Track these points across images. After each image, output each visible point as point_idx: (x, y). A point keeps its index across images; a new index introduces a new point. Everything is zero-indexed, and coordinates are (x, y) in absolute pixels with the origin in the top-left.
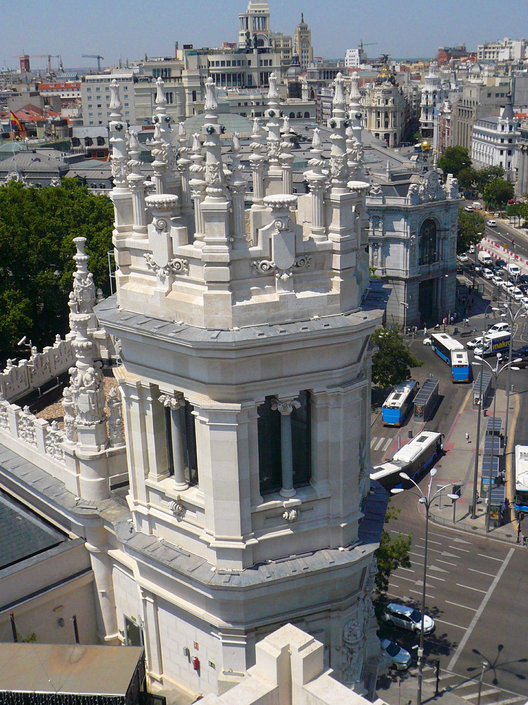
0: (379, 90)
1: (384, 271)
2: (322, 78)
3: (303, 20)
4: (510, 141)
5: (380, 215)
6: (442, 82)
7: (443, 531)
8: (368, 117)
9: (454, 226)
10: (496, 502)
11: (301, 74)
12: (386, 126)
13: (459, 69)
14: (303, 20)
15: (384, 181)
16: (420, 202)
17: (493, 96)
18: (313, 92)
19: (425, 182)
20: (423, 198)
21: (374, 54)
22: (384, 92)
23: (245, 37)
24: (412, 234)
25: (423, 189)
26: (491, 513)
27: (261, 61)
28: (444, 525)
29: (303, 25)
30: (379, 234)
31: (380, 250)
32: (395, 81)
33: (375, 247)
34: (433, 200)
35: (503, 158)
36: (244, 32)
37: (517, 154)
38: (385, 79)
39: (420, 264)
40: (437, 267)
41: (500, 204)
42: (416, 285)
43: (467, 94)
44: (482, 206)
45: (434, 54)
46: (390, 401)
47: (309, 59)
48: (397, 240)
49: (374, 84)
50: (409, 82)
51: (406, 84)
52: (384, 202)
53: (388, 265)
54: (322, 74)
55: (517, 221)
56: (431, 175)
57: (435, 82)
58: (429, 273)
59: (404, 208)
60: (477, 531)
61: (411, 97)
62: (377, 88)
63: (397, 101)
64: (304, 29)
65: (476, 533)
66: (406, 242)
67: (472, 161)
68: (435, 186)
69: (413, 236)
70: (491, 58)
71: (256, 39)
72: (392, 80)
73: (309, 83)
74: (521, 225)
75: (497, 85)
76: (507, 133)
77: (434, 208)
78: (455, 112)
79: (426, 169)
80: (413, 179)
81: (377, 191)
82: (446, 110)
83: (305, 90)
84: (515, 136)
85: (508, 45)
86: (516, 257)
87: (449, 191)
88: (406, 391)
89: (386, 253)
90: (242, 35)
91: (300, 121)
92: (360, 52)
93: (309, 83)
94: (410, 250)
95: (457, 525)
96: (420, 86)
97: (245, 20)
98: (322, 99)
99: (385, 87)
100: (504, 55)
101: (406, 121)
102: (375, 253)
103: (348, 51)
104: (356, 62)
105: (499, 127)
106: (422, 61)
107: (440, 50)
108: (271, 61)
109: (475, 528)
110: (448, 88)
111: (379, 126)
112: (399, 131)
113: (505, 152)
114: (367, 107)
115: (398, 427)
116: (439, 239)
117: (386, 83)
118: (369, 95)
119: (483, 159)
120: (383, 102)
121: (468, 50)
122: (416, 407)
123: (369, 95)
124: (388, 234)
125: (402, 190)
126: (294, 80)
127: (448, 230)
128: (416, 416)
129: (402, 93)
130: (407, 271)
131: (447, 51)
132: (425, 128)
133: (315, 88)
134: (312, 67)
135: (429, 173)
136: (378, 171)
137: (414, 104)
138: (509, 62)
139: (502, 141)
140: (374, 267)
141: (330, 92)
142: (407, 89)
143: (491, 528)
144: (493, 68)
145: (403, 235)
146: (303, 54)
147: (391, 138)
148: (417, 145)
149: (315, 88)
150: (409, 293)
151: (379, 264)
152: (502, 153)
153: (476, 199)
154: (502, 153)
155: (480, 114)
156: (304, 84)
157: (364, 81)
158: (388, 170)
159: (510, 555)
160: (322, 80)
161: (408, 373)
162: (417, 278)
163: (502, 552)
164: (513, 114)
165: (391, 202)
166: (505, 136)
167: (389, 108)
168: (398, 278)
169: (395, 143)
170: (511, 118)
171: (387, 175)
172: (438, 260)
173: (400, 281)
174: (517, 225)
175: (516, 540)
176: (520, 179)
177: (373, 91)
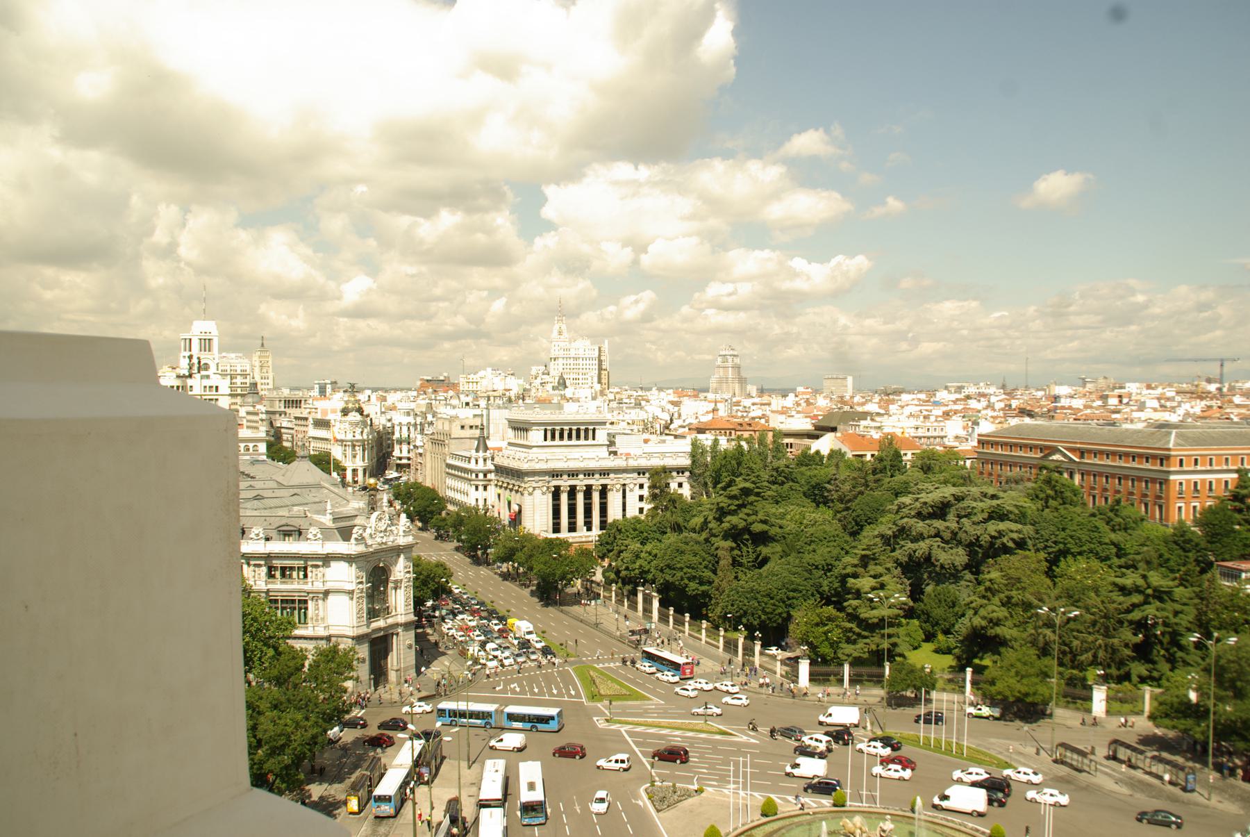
3: (263, 345)
4: (485, 476)
5: (320, 563)
13: (436, 400)
14: (263, 345)
15: (325, 525)
17: (467, 427)
18: (271, 423)
22: (351, 424)
23: (187, 360)
27: (205, 387)
30: (319, 586)
32: (363, 412)
35: (481, 494)
36: (187, 354)
37: (491, 488)
49: (340, 414)
50: (382, 413)
53: (330, 621)
54: (283, 402)
59: (347, 555)
62: (343, 419)
71: (199, 362)
80: (358, 521)
81: (315, 535)
82: (418, 443)
87: (401, 533)
90: (184, 357)
97: (188, 341)
105: (473, 461)
107: (422, 380)
108: (217, 387)
113: (481, 488)
124: (328, 586)
125: (346, 534)
132: (398, 462)
136: (318, 512)
138: (491, 393)
139: (477, 476)
152: (477, 488)
154: (477, 488)
157: (329, 412)
158: (329, 511)
167: (357, 441)
171: (329, 517)
173: (345, 639)
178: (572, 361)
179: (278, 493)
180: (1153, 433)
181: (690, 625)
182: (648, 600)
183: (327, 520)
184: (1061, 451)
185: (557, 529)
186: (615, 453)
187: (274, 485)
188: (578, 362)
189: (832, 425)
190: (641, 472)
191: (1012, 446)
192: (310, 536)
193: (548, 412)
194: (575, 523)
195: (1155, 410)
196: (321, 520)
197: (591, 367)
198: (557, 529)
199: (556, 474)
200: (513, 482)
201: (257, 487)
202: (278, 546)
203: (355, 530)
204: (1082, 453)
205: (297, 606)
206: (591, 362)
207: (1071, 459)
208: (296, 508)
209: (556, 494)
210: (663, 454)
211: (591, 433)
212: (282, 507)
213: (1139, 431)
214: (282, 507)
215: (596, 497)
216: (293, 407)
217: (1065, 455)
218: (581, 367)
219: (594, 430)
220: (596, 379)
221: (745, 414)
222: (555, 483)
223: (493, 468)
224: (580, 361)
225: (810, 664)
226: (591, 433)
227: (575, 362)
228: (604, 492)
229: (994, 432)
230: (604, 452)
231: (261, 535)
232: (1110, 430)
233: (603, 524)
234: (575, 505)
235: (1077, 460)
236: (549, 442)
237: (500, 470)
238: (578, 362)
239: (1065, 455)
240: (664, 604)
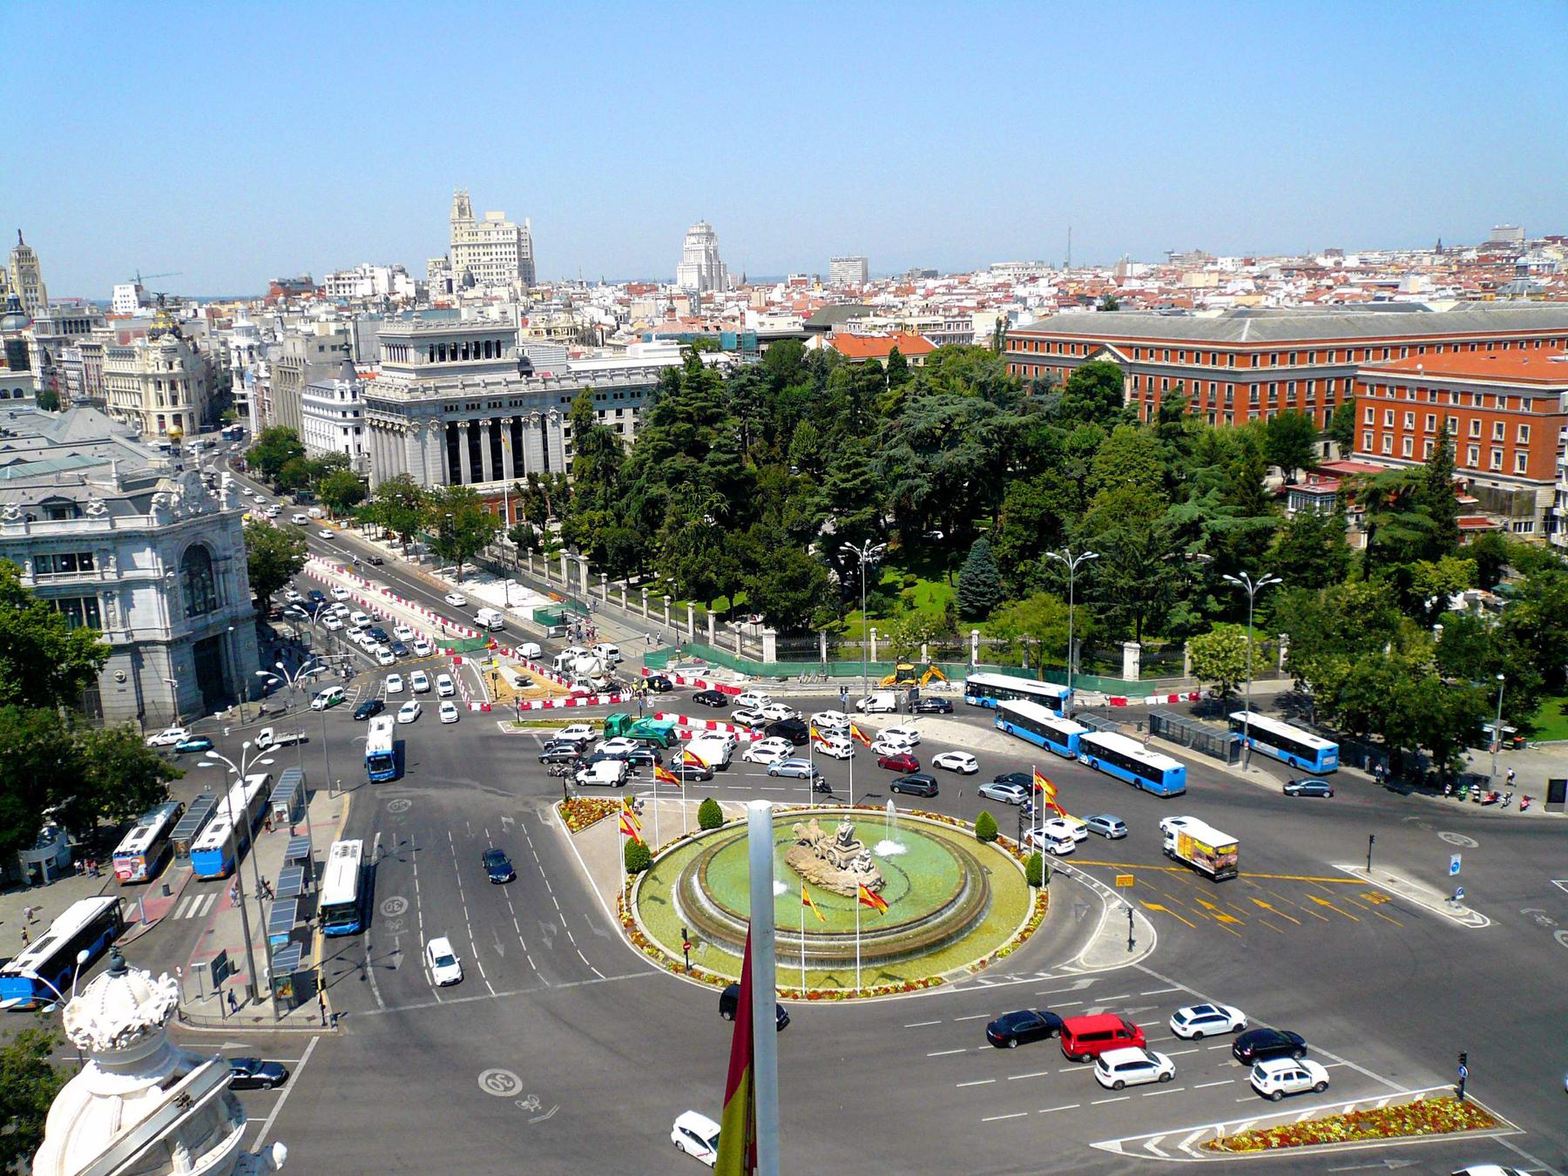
0: (156, 348)
1: (129, 634)
2: (62, 332)
4: (356, 414)
6: (262, 332)
7: (191, 1036)
8: (143, 391)
9: (239, 550)
10: (284, 969)
11: (24, 327)
12: (174, 401)
13: (288, 312)
16: (176, 520)
17: (328, 349)
19: (180, 488)
20: (179, 513)
21: (152, 289)
22: (164, 350)
24: (166, 571)
25: (177, 499)
26: (281, 988)
28: (207, 1026)
29: (22, 248)
30: (111, 576)
31: (117, 601)
32: (181, 333)
33: (109, 598)
34: (197, 514)
35: (350, 439)
38: (163, 331)
39: (190, 616)
40: (220, 617)
41: (347, 507)
42: (187, 649)
43: (289, 350)
44: (324, 514)
45: (264, 290)
46: (126, 845)
47: (39, 303)
48: (143, 583)
50: (212, 333)
51: (207, 336)
52: (113, 525)
53: (134, 625)
54: (61, 326)
55: (373, 530)
56: (188, 476)
57: (248, 331)
58: (207, 628)
60: (261, 1023)
61: (217, 355)
62: (152, 345)
63: (187, 364)
64: (24, 255)
65: (258, 1027)
66: (159, 584)
67: (307, 447)
68: (197, 494)
69: (170, 574)
70: (347, 294)
72: (175, 332)
73: (40, 341)
74: (380, 535)
75: (332, 333)
76: (350, 403)
77: (199, 528)
78: (275, 375)
79: (180, 468)
80: (162, 485)
81: (98, 510)
82: (263, 374)
83: (34, 352)
84: (363, 407)
85: (368, 274)
86: (368, 584)
87: (223, 498)
88: (160, 819)
89: (128, 604)
91: (6, 403)
92: (138, 289)
93: (40, 341)
94: (168, 595)
95: (229, 1021)
96: (229, 339)
98: (65, 365)
99: (166, 344)
100: (363, 289)
101: (209, 393)
102: (110, 607)
103: (117, 288)
104: (131, 304)
106: (243, 300)
107: (272, 283)
109: (257, 1019)
110: (272, 341)
111: (162, 404)
112: (196, 408)
114: (139, 376)
115: (149, 881)
116: (217, 573)
117: (166, 336)
118: (140, 356)
119: (321, 443)
120: (164, 366)
121: (315, 283)
122: (176, 844)
123: (140, 356)
124: (128, 575)
125: (142, 505)
126: (15, 337)
127: (230, 558)
128: (178, 858)
129: (196, 351)
130: (167, 629)
131: (282, 284)
133: (50, 348)
134: (41, 315)
135: (183, 474)
137: (223, 366)
139: (344, 414)
140: (112, 629)
141: (76, 354)
142: (208, 345)
143: (282, 1013)
144: (333, 309)
145: (152, 575)
146: (28, 295)
147: (185, 421)
148: (228, 430)
149: (50, 348)
150: (176, 663)
151: (119, 625)
153: (314, 503)
154: (346, 431)
155: (310, 377)
156: (32, 342)
159: (309, 1050)
160: (62, 335)
161: (163, 791)
162: (187, 638)
163: (298, 1045)
164: (355, 375)
165: (125, 524)
166: (347, 406)
168: (154, 643)
169: (192, 427)
170: (352, 381)
171: (115, 483)
172: (221, 605)
174: (373, 537)
175: (321, 1022)
176: (374, 468)
177: (146, 349)
178: (481, 250)
179: (47, 454)
180: (1223, 324)
181: (628, 596)
182: (574, 565)
183: (111, 488)
184: (1110, 351)
185: (456, 477)
186: (529, 373)
187: (43, 443)
188: (489, 250)
189: (827, 324)
190: (564, 398)
191: (1049, 345)
192: (90, 511)
193: (432, 322)
194: (480, 471)
195: (1249, 293)
196: (107, 488)
197: (508, 256)
198: (456, 477)
199: (450, 406)
200: (392, 419)
201: (18, 448)
202: (47, 528)
203: (155, 498)
204: (1137, 351)
205: (81, 606)
206: (508, 250)
207: (1121, 359)
208: (64, 474)
209: (452, 436)
210: (595, 374)
211: (494, 347)
212: (48, 474)
213: (1208, 321)
214: (48, 474)
215: (506, 437)
216: (77, 332)
217: (1114, 354)
218: (494, 256)
219: (498, 344)
220: (515, 273)
221: (716, 314)
222: (450, 417)
223: (364, 402)
224: (494, 249)
225: (777, 637)
226: (494, 347)
227: (486, 251)
228: (517, 429)
229: (1028, 327)
230: (514, 375)
231: (19, 515)
232: (1170, 321)
233: (519, 472)
234: (478, 446)
235: (1129, 361)
236: (436, 364)
237: (374, 404)
238: (489, 250)
239: (1114, 354)
240: (591, 570)
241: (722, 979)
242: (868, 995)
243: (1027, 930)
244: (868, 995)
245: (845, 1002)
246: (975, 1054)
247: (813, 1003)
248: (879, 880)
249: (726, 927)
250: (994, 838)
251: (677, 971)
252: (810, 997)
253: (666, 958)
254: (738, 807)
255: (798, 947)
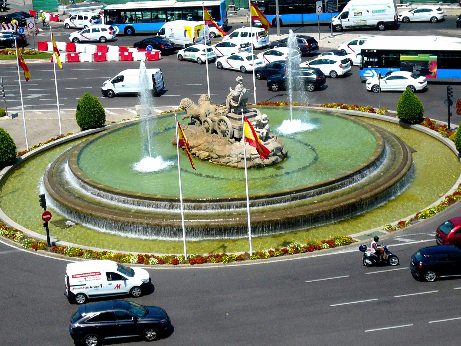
241: (90, 252)
242: (262, 256)
243: (455, 194)
244: (262, 256)
245: (235, 264)
246: (389, 302)
247: (196, 267)
248: (280, 149)
249: (99, 204)
250: (420, 121)
251: (36, 247)
252: (193, 261)
253: (25, 237)
254: (126, 112)
255: (177, 216)
